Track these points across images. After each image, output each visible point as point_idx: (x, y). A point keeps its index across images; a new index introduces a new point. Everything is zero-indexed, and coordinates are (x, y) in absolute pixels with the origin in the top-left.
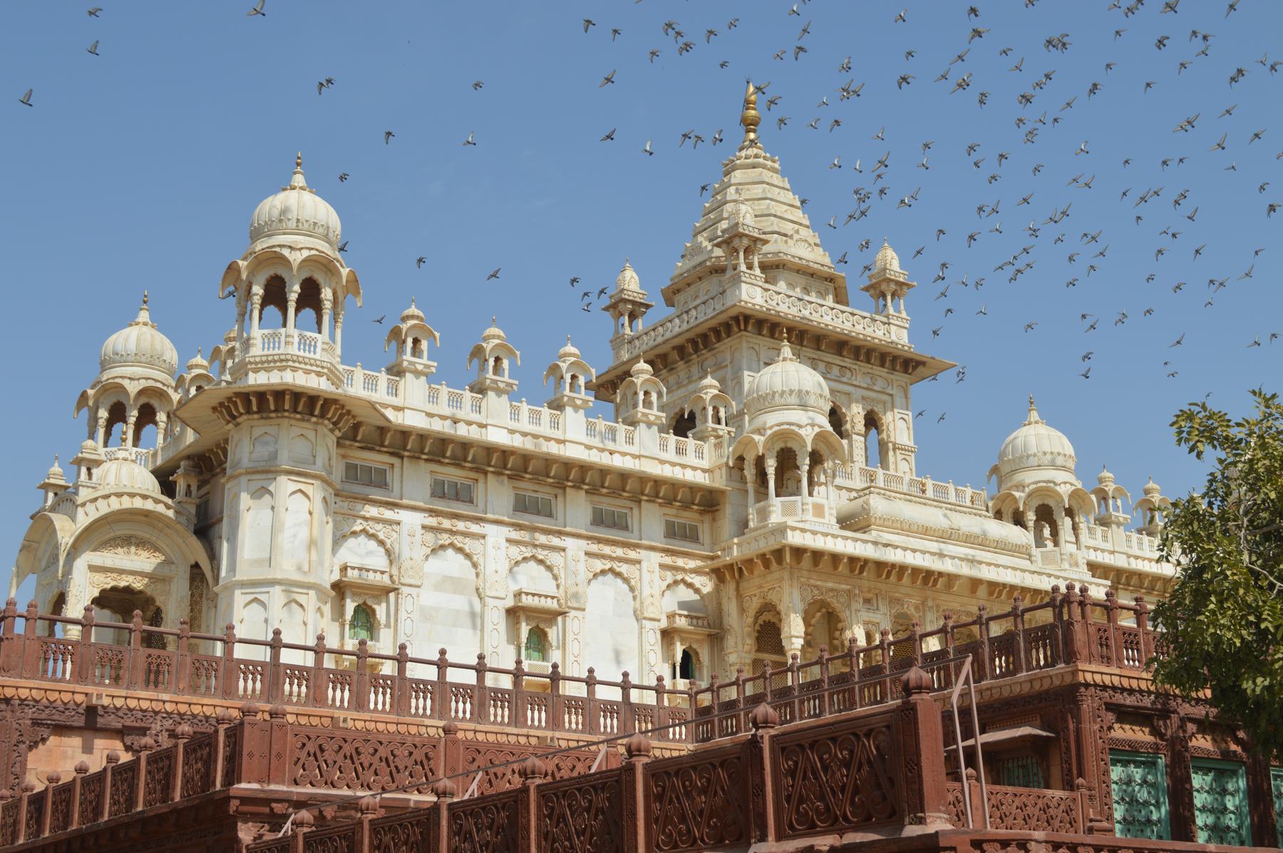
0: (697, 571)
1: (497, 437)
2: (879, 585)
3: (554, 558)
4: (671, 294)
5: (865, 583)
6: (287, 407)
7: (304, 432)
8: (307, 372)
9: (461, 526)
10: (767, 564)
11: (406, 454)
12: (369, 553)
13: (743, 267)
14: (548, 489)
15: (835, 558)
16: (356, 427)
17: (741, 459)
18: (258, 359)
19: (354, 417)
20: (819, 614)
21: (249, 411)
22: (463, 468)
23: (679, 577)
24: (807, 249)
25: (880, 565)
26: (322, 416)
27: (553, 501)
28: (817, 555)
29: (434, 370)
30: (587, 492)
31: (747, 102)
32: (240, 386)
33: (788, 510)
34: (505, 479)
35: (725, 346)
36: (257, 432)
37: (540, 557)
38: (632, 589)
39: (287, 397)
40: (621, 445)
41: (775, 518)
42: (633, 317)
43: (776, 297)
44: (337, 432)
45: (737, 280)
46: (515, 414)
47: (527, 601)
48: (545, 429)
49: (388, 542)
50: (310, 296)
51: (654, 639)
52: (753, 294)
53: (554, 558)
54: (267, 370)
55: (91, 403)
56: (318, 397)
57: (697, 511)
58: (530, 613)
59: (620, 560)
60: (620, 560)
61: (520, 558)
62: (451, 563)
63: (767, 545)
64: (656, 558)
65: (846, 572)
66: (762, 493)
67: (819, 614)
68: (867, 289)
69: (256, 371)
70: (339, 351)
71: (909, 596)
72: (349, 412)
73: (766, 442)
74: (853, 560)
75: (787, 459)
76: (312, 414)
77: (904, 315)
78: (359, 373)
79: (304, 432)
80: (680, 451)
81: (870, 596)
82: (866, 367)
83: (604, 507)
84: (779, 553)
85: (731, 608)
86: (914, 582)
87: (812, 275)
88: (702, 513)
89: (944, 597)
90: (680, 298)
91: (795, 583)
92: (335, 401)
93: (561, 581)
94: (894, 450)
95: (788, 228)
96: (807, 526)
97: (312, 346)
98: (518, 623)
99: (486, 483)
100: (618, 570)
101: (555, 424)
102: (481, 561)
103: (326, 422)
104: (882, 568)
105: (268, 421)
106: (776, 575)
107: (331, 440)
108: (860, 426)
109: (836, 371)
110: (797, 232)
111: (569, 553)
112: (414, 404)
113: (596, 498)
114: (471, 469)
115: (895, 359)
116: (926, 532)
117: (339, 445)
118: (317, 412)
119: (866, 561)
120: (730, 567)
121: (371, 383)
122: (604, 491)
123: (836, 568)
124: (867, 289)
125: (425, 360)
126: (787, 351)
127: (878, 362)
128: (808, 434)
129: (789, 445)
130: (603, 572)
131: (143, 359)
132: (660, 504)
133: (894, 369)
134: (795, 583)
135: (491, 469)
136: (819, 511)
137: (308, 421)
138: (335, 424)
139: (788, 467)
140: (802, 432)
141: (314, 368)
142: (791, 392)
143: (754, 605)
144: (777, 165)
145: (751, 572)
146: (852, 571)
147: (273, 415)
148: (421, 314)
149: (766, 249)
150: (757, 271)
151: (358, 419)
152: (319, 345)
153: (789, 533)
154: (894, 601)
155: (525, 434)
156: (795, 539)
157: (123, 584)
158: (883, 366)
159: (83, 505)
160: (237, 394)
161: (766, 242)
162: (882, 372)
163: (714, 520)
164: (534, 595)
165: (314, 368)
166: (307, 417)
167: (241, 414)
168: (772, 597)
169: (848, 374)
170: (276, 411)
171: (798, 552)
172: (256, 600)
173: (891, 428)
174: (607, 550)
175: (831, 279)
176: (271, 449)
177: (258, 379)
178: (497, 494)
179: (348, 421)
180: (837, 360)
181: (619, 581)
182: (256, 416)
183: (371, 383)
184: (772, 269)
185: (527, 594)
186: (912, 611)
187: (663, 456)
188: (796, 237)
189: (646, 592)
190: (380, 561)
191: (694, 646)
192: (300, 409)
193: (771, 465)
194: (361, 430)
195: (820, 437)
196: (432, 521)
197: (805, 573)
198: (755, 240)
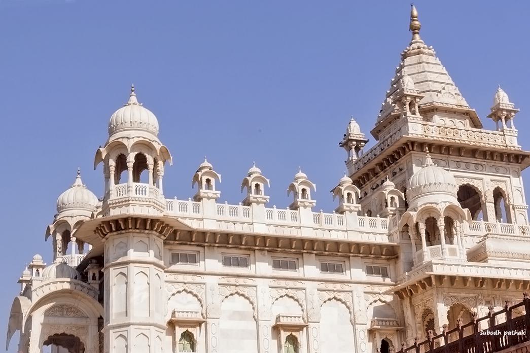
0: (385, 293)
1: (260, 229)
2: (495, 292)
3: (299, 295)
4: (376, 133)
5: (485, 292)
6: (130, 227)
7: (143, 239)
8: (141, 205)
9: (241, 281)
10: (424, 287)
11: (206, 244)
12: (189, 302)
13: (409, 114)
14: (293, 256)
15: (464, 279)
16: (175, 232)
17: (407, 226)
18: (114, 202)
19: (172, 227)
20: (462, 312)
21: (111, 231)
22: (241, 249)
23: (377, 298)
24: (451, 97)
25: (493, 281)
27: (296, 262)
28: (452, 279)
29: (219, 196)
30: (316, 255)
31: (412, 16)
32: (107, 218)
33: (433, 254)
34: (266, 252)
35: (403, 160)
36: (117, 242)
37: (290, 295)
38: (348, 307)
39: (130, 221)
40: (335, 225)
41: (427, 258)
42: (357, 149)
43: (431, 128)
44: (162, 237)
45: (406, 122)
46: (270, 216)
47: (284, 321)
48: (288, 221)
49: (199, 295)
50: (141, 164)
51: (363, 335)
52: (416, 129)
54: (120, 207)
55: (51, 232)
56: (148, 219)
57: (385, 259)
58: (286, 327)
59: (339, 291)
60: (339, 291)
61: (278, 297)
62: (239, 303)
63: (421, 276)
64: (362, 288)
65: (473, 286)
66: (419, 245)
67: (462, 312)
68: (490, 116)
69: (114, 208)
70: (161, 191)
71: (515, 296)
72: (167, 225)
73: (418, 215)
74: (475, 279)
75: (431, 224)
76: (145, 229)
77: (514, 128)
78: (176, 202)
79: (143, 239)
80: (372, 225)
81: (489, 299)
82: (492, 163)
83: (328, 262)
84: (429, 279)
85: (408, 313)
86: (517, 288)
87: (455, 112)
88: (388, 260)
90: (380, 135)
91: (440, 295)
92: (158, 220)
93: (304, 307)
94: (514, 209)
95: (438, 87)
96: (444, 262)
97: (144, 191)
98: (280, 333)
99: (255, 256)
100: (338, 298)
101: (295, 218)
102: (255, 301)
103: (154, 232)
104: (495, 283)
105: (121, 234)
106: (429, 292)
107: (160, 242)
108: (491, 198)
109: (472, 166)
110: (444, 89)
111: (308, 291)
112: (208, 215)
113: (322, 258)
114: (245, 249)
115: (509, 155)
117: (165, 243)
118: (148, 228)
119: (484, 279)
120: (404, 290)
121: (183, 208)
122: (326, 253)
123: (465, 285)
124: (490, 116)
125: (214, 191)
126: (429, 160)
127: (499, 159)
128: (442, 207)
129: (432, 216)
130: (330, 299)
131: (78, 205)
132: (362, 257)
133: (510, 162)
134: (440, 295)
135: (257, 248)
136: (453, 252)
137: (143, 233)
138: (161, 232)
139: (434, 230)
140: (438, 207)
141: (145, 203)
142: (437, 184)
143: (420, 311)
144: (431, 52)
145: (417, 291)
146: (476, 285)
147: (123, 232)
148: (210, 165)
149: (422, 101)
150: (418, 115)
151: (176, 228)
152: (147, 190)
153: (434, 266)
155: (277, 226)
156: (438, 270)
157: (60, 332)
158: (502, 160)
159: (35, 290)
160: (103, 222)
161: (421, 98)
162: (503, 164)
163: (396, 263)
164: (287, 317)
165: (145, 203)
166: (142, 231)
167: (108, 233)
168: (429, 305)
169: (481, 168)
170: (125, 229)
171: (440, 278)
172: (121, 335)
173: (511, 196)
174: (330, 286)
175: (466, 114)
176: (124, 251)
177: (115, 213)
179: (168, 230)
180: (473, 161)
181: (339, 302)
182: (115, 233)
183: (183, 208)
184: (428, 112)
185: (283, 317)
187: (362, 229)
188: (443, 91)
189: (357, 308)
190: (195, 306)
191: (389, 337)
192: (138, 227)
193: (422, 228)
194: (178, 233)
195: (450, 208)
197: (446, 290)
198: (415, 97)
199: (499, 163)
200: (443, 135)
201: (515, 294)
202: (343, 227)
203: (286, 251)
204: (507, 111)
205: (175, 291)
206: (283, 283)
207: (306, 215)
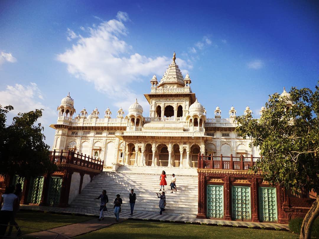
2: (143, 140)
26: (61, 127)
30: (107, 130)
58: (95, 149)
81: (141, 141)
82: (178, 98)
89: (158, 140)
109: (171, 100)
116: (156, 128)
130: (109, 142)
154: (145, 142)
162: (182, 98)
174: (110, 138)
186: (151, 143)
199: (180, 98)
201: (150, 140)
202: (117, 122)
203: (99, 130)
204: (187, 81)
205: (71, 141)
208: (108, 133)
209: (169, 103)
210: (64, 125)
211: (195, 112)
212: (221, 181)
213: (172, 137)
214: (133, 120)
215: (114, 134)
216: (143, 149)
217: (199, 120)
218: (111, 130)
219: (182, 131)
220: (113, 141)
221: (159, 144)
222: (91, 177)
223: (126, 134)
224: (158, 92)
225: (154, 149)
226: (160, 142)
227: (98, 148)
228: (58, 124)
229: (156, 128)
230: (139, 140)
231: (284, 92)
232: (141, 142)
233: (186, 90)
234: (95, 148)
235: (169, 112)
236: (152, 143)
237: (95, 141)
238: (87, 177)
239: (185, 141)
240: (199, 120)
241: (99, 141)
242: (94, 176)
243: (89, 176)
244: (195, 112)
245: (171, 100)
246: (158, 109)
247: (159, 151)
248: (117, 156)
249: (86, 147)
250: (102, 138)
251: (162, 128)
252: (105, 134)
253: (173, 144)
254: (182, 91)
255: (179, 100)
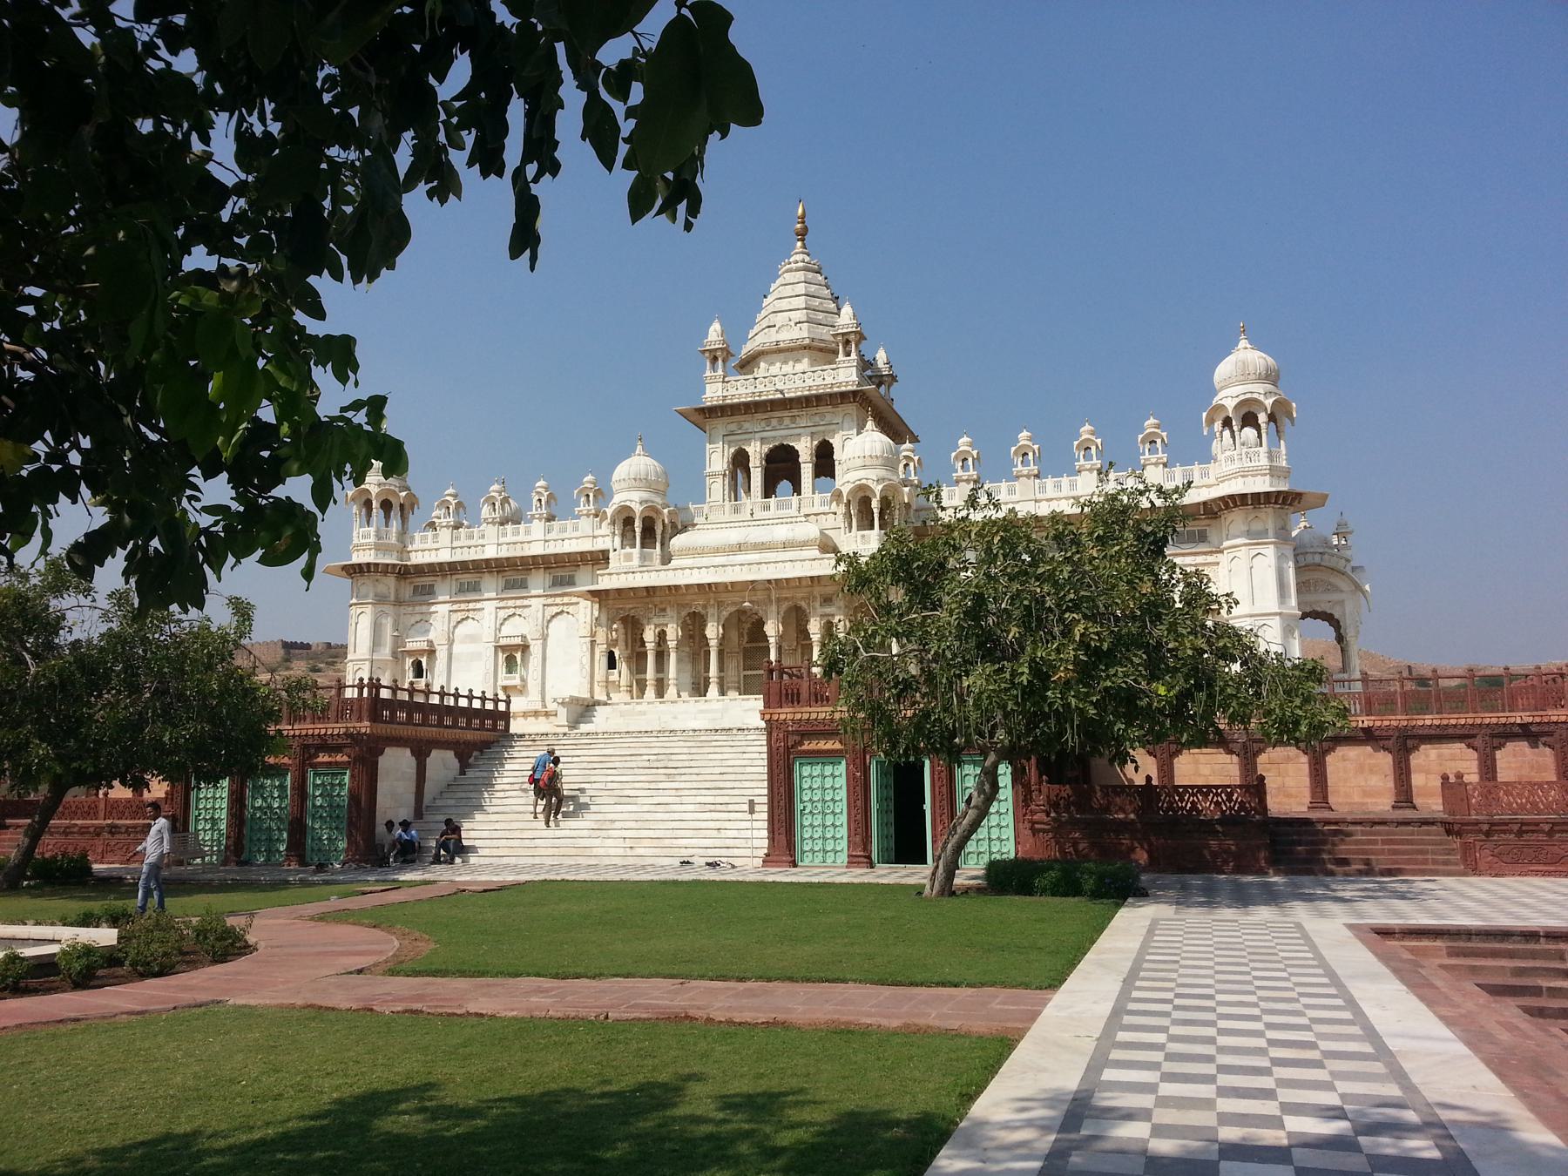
53: (526, 612)
58: (503, 648)
109: (787, 421)
116: (717, 551)
154: (681, 606)
178: (491, 586)
180: (786, 413)
186: (700, 609)
189: (581, 617)
196: (455, 607)
199: (822, 409)
200: (752, 389)
203: (512, 573)
206: (510, 603)
207: (538, 528)
208: (548, 580)
209: (779, 436)
210: (377, 565)
211: (862, 474)
212: (838, 746)
213: (776, 580)
214: (628, 522)
215: (571, 583)
216: (673, 632)
217: (875, 504)
218: (562, 569)
219: (816, 553)
220: (570, 609)
221: (732, 609)
222: (459, 756)
223: (606, 582)
224: (732, 391)
225: (712, 631)
226: (734, 603)
227: (518, 641)
228: (358, 558)
229: (717, 551)
230: (657, 600)
231: (1243, 343)
232: (664, 610)
233: (845, 375)
234: (503, 642)
235: (782, 467)
236: (705, 607)
237: (502, 614)
238: (442, 763)
239: (830, 590)
240: (875, 504)
241: (518, 611)
242: (475, 753)
243: (450, 755)
244: (862, 474)
245: (787, 421)
246: (740, 461)
247: (741, 635)
248: (588, 667)
249: (473, 638)
250: (526, 602)
251: (740, 548)
252: (538, 583)
253: (785, 606)
254: (829, 380)
255: (817, 419)
